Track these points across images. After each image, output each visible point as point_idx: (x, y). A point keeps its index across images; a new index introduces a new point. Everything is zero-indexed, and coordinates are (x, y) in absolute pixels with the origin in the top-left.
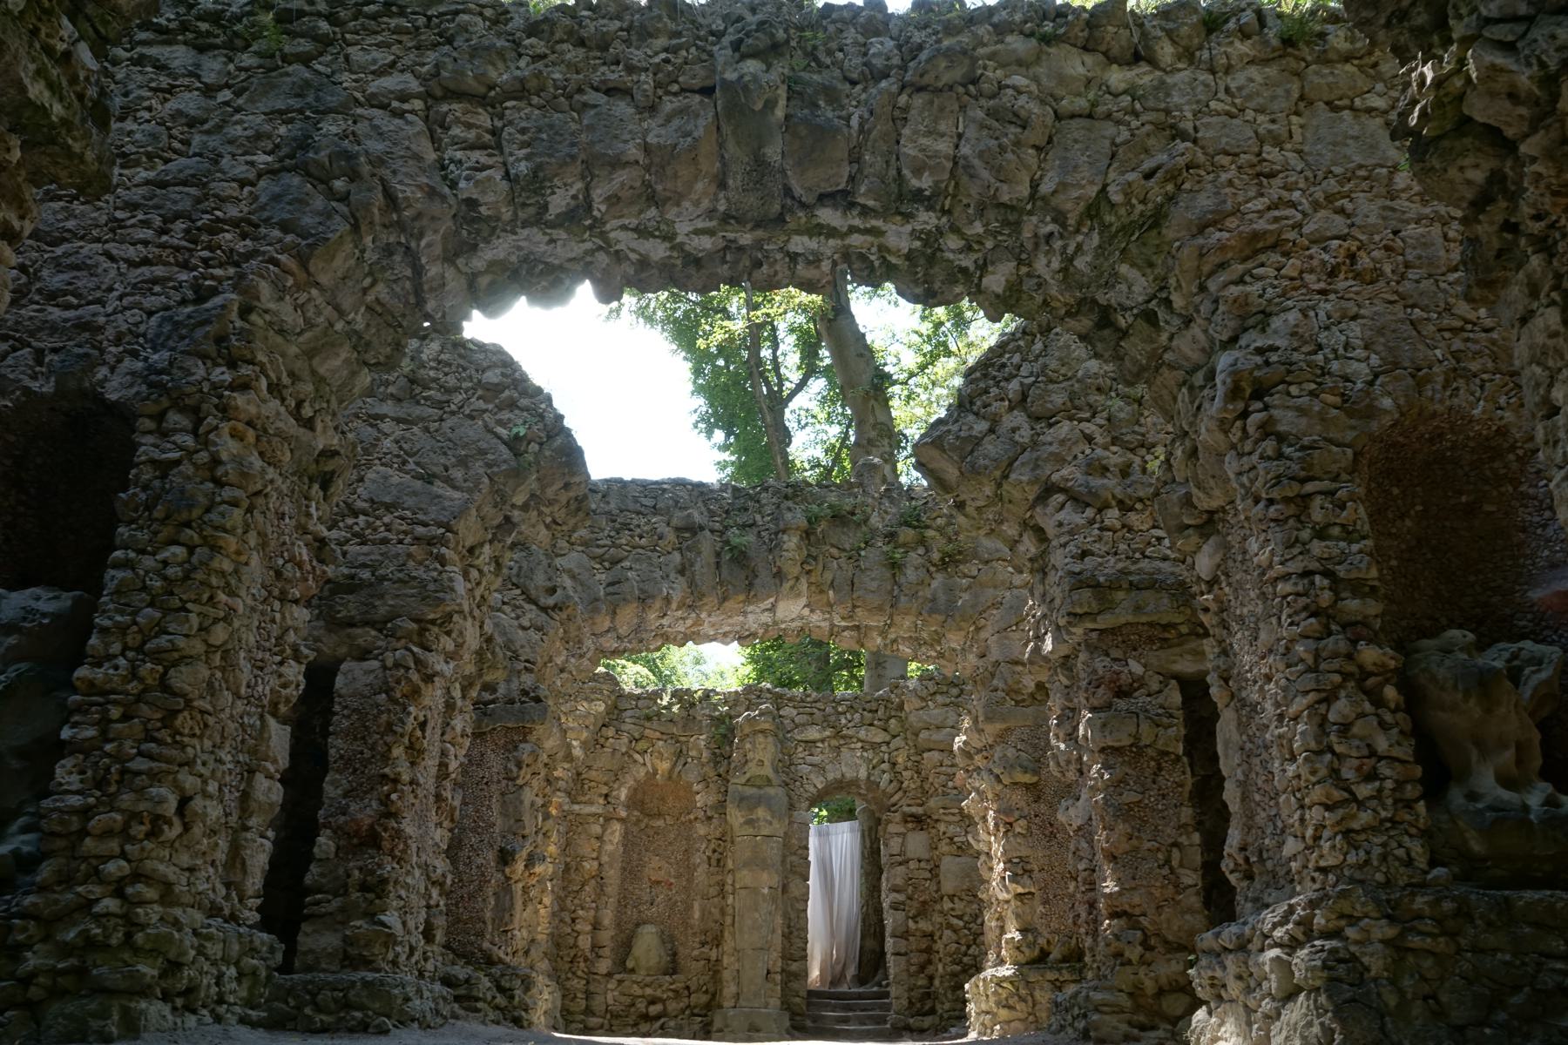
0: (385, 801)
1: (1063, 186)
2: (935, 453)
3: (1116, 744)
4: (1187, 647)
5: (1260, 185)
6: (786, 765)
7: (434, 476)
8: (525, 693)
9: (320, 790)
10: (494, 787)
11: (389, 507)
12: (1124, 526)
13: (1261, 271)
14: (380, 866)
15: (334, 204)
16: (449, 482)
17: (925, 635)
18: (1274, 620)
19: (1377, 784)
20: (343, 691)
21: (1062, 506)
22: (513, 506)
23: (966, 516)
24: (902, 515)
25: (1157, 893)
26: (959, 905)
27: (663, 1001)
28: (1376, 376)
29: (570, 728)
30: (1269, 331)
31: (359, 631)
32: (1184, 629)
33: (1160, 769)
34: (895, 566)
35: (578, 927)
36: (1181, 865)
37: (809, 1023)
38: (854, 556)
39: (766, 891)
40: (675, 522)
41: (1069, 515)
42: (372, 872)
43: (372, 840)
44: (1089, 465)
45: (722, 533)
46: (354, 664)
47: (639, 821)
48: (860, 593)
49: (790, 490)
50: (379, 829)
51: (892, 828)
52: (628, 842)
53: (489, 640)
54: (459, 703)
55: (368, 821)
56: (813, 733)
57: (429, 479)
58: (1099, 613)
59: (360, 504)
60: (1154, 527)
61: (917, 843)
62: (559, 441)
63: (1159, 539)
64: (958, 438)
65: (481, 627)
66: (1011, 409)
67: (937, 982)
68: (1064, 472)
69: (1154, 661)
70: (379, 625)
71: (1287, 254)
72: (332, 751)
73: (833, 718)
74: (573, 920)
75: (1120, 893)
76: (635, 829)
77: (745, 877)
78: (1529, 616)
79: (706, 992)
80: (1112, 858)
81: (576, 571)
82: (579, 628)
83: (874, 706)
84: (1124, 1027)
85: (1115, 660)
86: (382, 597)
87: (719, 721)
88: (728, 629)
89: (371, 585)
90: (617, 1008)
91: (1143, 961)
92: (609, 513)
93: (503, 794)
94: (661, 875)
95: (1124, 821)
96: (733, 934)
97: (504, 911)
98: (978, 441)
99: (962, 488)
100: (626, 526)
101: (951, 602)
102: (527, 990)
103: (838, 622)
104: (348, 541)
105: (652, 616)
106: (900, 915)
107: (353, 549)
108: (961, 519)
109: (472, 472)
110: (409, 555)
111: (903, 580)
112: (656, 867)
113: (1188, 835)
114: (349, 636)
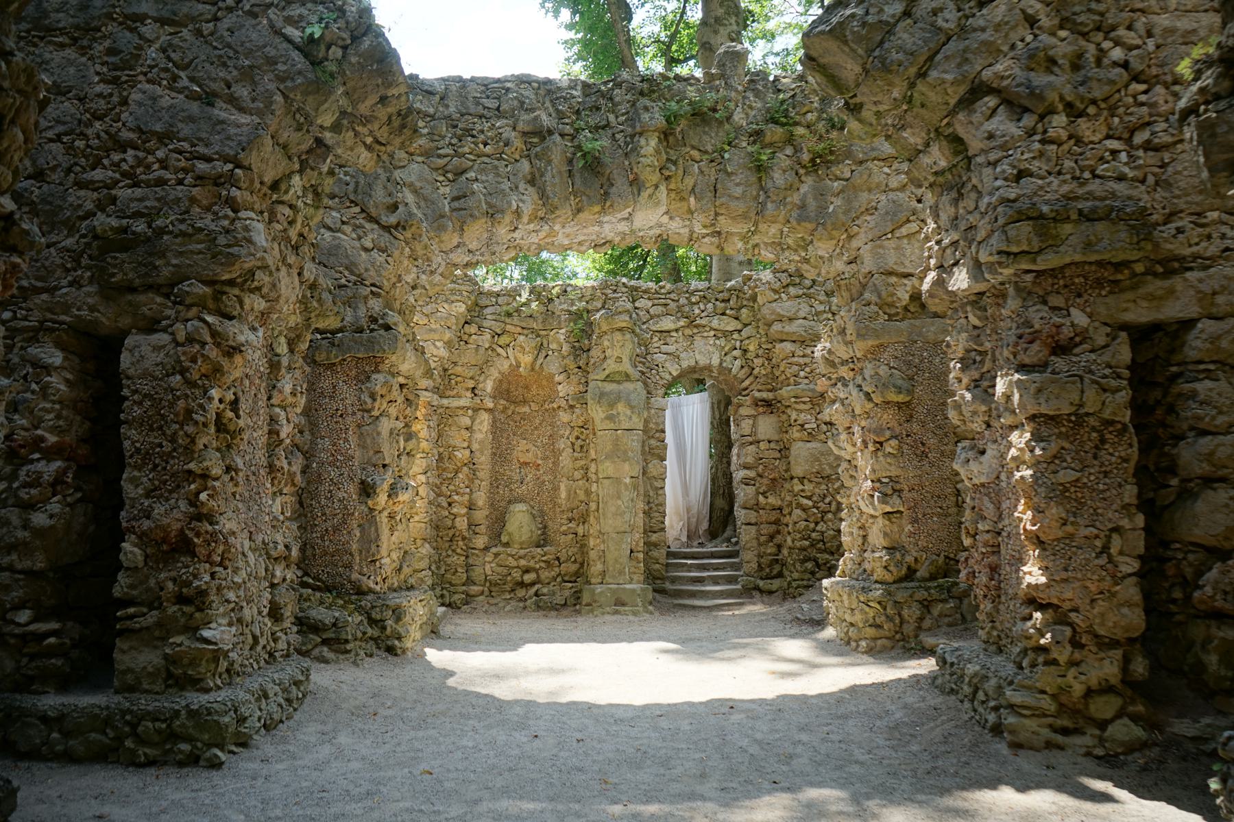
0: (193, 501)
2: (832, 45)
3: (1052, 413)
4: (1140, 291)
6: (643, 358)
7: (215, 95)
8: (373, 320)
9: (120, 490)
10: (349, 419)
11: (164, 137)
12: (1070, 137)
14: (195, 576)
16: (233, 101)
17: (790, 241)
20: (131, 372)
21: (994, 111)
22: (321, 127)
23: (860, 121)
24: (768, 110)
25: (1093, 588)
26: (808, 487)
27: (536, 571)
29: (431, 330)
31: (142, 298)
32: (1139, 268)
33: (1103, 441)
34: (760, 169)
35: (455, 510)
36: (1121, 553)
37: (668, 586)
38: (717, 159)
39: (628, 480)
40: (520, 126)
41: (1003, 124)
42: (188, 584)
43: (184, 547)
44: (1031, 57)
45: (573, 137)
46: (140, 338)
47: (506, 408)
48: (723, 200)
49: (645, 86)
50: (190, 534)
51: (744, 411)
52: (497, 430)
53: (313, 286)
54: (285, 362)
55: (176, 526)
56: (667, 323)
57: (208, 99)
58: (1040, 251)
59: (126, 135)
60: (1108, 137)
61: (766, 426)
62: (366, 43)
63: (1114, 153)
64: (864, 24)
65: (299, 274)
67: (785, 552)
68: (999, 67)
69: (1102, 310)
70: (167, 289)
72: (127, 444)
73: (687, 309)
74: (450, 504)
75: (1047, 586)
76: (502, 417)
77: (608, 468)
79: (575, 561)
80: (1039, 541)
81: (418, 184)
82: (426, 247)
83: (725, 295)
84: (1046, 733)
85: (1053, 309)
86: (162, 255)
87: (577, 316)
88: (582, 238)
89: (149, 239)
90: (495, 578)
91: (1073, 663)
92: (449, 117)
93: (359, 426)
94: (528, 457)
95: (1058, 504)
96: (598, 519)
97: (370, 541)
98: (888, 29)
99: (863, 89)
100: (468, 132)
101: (822, 208)
102: (398, 619)
103: (699, 229)
104: (118, 182)
105: (502, 231)
106: (750, 490)
107: (123, 193)
108: (853, 125)
109: (260, 89)
110: (193, 200)
111: (770, 184)
112: (524, 450)
113: (1131, 517)
114: (130, 303)
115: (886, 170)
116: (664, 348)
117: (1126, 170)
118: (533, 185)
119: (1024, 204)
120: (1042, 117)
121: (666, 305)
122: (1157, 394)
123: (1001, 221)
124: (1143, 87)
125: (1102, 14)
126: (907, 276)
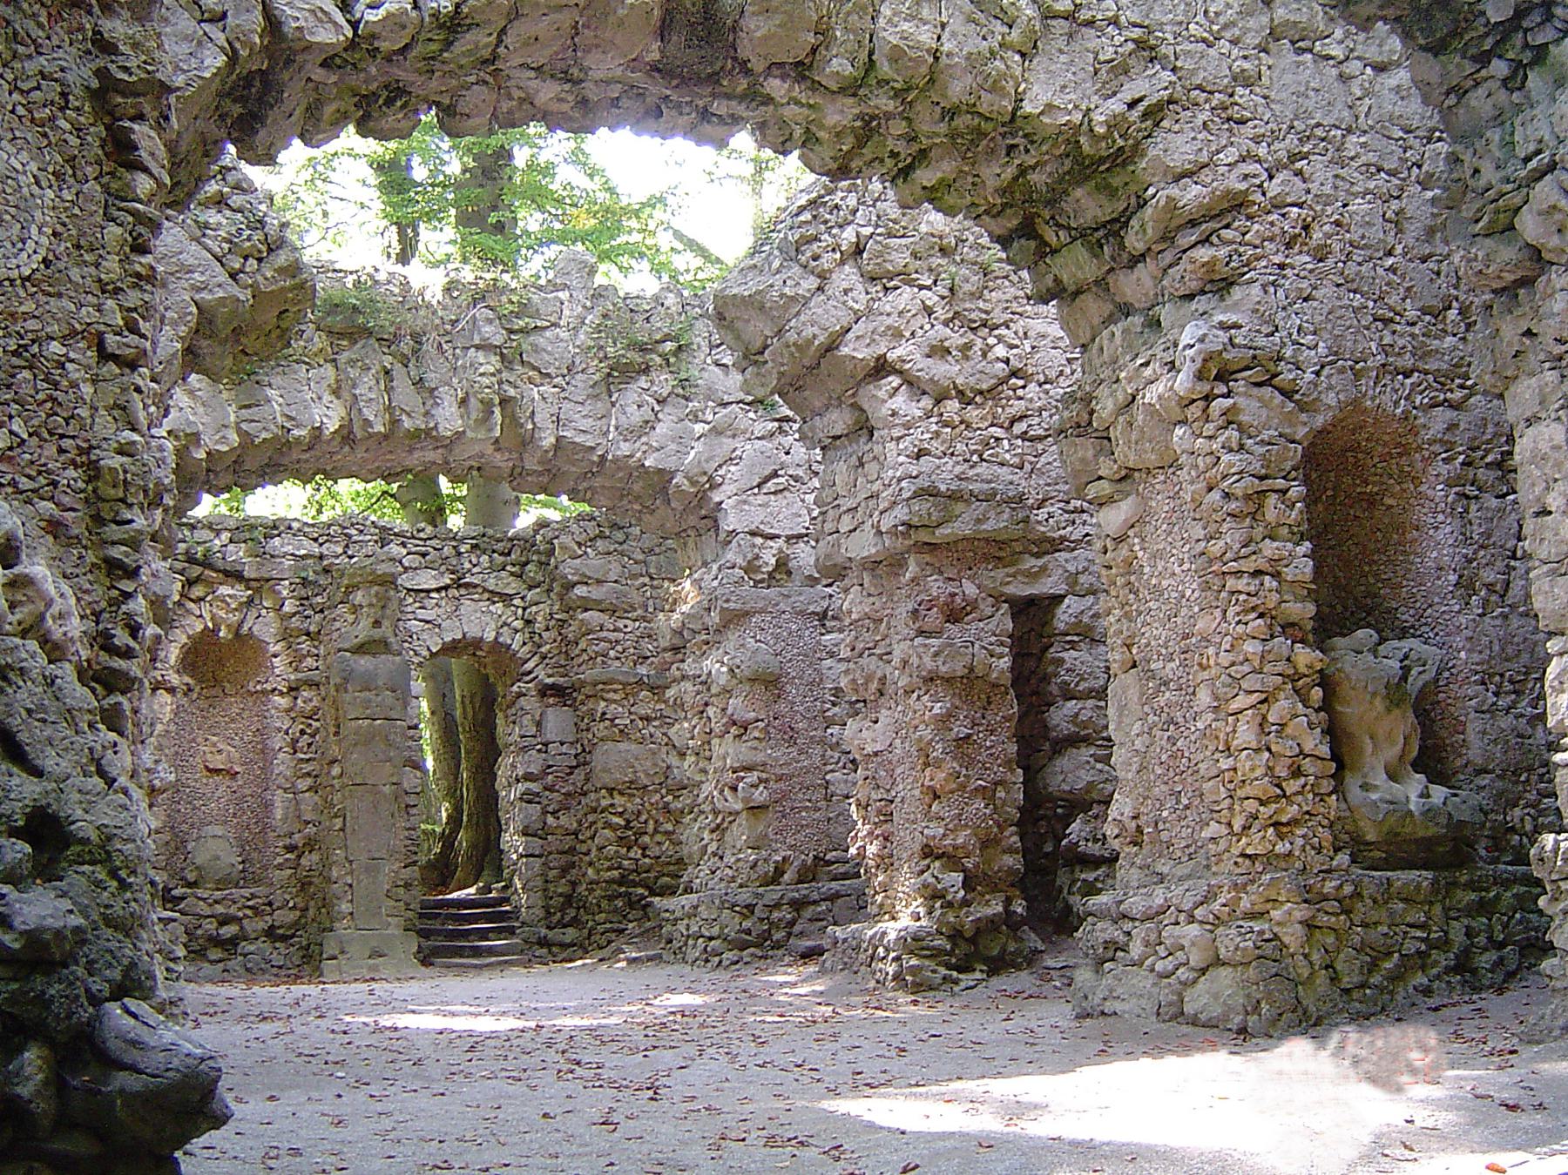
1: (1049, 107)
5: (1230, 130)
13: (1227, 234)
15: (206, 27)
18: (1218, 613)
19: (1303, 780)
21: (897, 389)
26: (618, 800)
28: (1322, 367)
30: (1229, 302)
56: (427, 580)
60: (992, 425)
61: (557, 721)
62: (282, 258)
66: (842, 262)
67: (582, 889)
68: (899, 352)
71: (1249, 217)
78: (1412, 612)
94: (218, 762)
109: (175, 298)
113: (1013, 771)
115: (751, 415)
116: (421, 614)
117: (1007, 456)
118: (338, 398)
119: (923, 482)
120: (938, 402)
121: (424, 555)
122: (1032, 663)
123: (906, 495)
124: (1021, 383)
125: (987, 312)
126: (773, 537)
